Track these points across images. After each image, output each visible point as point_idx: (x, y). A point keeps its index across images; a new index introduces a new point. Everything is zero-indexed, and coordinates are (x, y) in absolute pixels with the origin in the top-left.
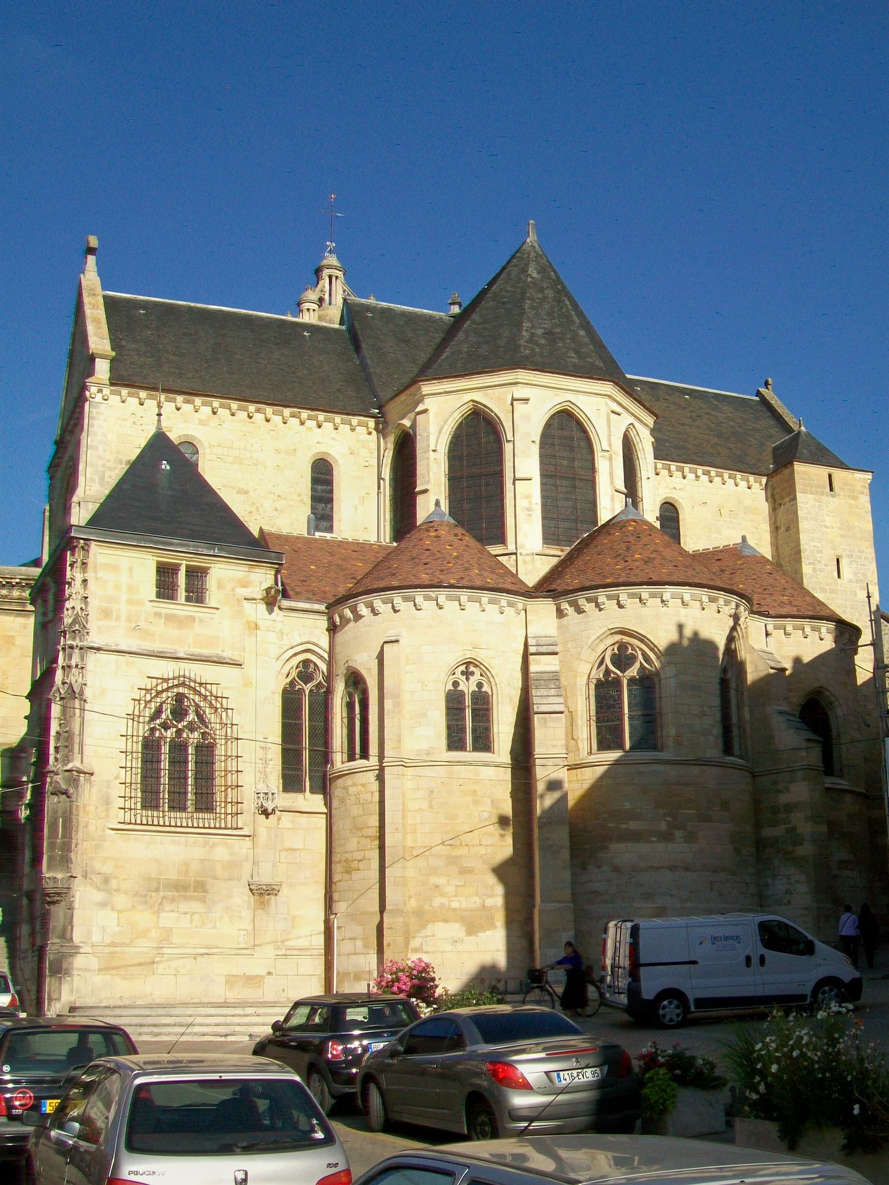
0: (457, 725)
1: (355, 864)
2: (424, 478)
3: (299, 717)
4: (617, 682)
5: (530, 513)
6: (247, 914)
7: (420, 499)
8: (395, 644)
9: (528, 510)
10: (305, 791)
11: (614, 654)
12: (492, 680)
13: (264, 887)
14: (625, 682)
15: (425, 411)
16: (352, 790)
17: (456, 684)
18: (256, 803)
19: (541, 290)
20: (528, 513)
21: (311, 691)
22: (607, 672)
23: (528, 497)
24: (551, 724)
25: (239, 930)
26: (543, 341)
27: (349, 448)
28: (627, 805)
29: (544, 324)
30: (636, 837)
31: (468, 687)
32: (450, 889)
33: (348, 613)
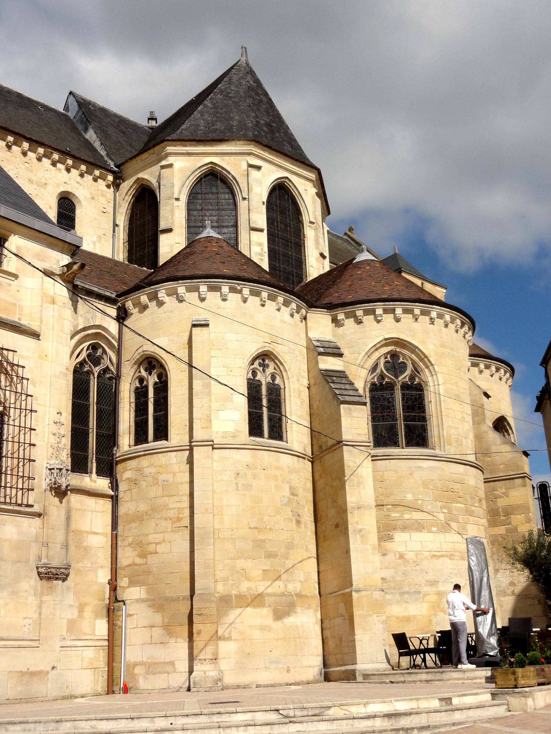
0: (256, 413)
1: (152, 548)
2: (167, 220)
3: (87, 398)
4: (390, 387)
5: (262, 258)
6: (32, 600)
7: (163, 239)
8: (205, 329)
9: (260, 255)
10: (91, 473)
11: (387, 362)
12: (284, 374)
13: (54, 571)
14: (398, 387)
15: (170, 166)
16: (147, 471)
17: (254, 373)
18: (47, 480)
19: (257, 94)
20: (260, 257)
21: (99, 373)
22: (382, 377)
23: (260, 245)
24: (354, 414)
25: (24, 618)
26: (265, 129)
27: (91, 194)
28: (410, 497)
29: (264, 117)
30: (419, 527)
31: (263, 378)
32: (257, 573)
33: (144, 299)
